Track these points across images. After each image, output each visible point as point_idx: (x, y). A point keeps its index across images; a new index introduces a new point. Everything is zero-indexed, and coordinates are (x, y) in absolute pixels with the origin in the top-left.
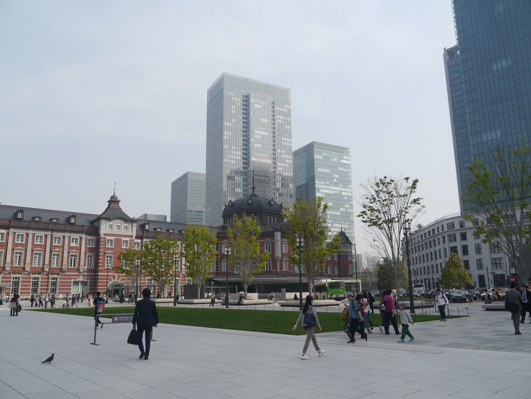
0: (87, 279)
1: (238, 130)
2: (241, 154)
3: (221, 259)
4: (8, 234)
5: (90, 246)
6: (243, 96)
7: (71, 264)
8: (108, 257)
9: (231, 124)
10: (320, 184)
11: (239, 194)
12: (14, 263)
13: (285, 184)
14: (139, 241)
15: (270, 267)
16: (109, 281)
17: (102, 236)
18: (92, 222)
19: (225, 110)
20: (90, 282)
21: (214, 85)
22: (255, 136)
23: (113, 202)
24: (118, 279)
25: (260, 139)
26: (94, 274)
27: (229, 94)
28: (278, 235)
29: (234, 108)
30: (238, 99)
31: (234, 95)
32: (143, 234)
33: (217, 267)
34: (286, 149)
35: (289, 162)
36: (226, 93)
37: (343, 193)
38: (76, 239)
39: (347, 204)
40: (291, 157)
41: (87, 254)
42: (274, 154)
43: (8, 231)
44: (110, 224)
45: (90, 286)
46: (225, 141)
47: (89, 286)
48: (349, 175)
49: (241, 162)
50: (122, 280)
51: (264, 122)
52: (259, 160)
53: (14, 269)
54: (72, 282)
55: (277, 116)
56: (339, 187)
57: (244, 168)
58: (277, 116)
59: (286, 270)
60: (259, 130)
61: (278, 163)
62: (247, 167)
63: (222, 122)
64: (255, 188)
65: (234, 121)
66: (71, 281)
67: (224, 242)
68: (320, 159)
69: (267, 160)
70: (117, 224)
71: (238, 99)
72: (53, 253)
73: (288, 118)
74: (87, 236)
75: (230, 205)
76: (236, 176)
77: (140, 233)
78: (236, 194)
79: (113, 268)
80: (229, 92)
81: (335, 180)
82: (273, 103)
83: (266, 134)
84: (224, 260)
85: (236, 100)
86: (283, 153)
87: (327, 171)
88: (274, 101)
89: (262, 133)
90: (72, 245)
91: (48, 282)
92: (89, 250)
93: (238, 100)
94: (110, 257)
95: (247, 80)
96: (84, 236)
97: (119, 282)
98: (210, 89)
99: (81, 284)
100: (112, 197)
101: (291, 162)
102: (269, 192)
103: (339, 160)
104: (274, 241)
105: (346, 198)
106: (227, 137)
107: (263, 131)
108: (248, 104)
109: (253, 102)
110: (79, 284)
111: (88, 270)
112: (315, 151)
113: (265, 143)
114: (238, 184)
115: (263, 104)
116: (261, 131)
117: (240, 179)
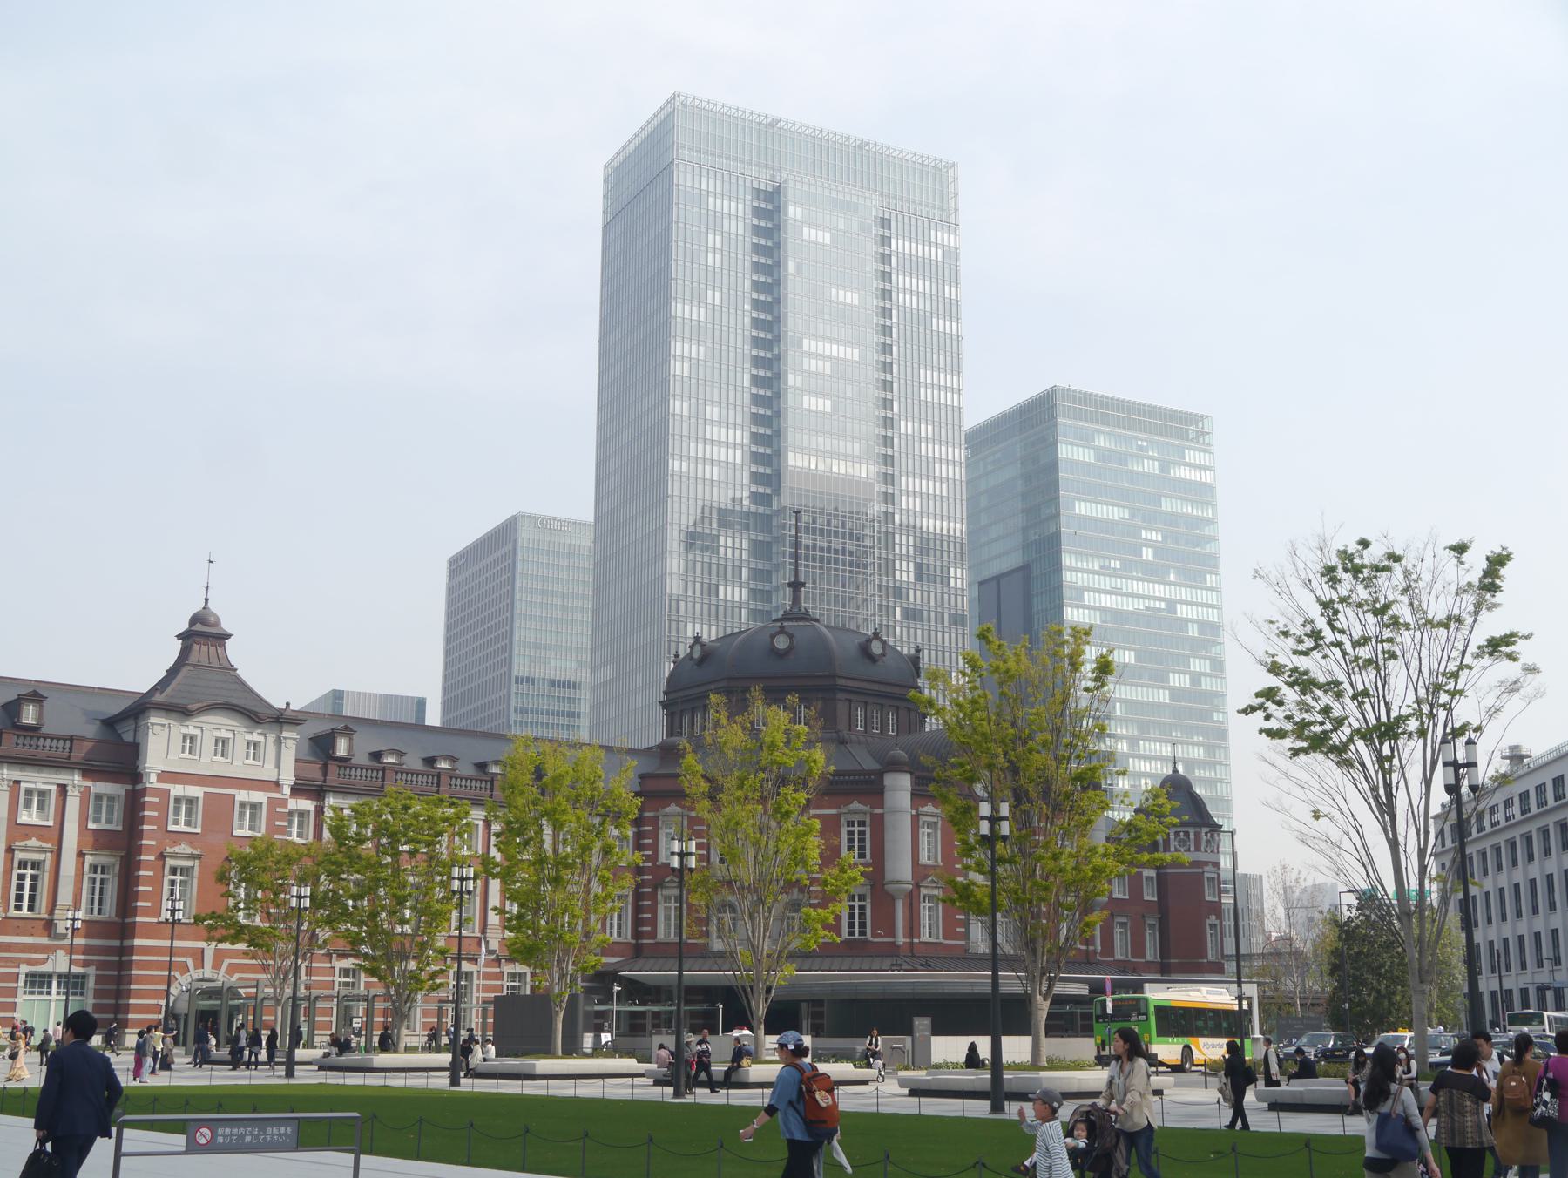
0: (86, 964)
1: (732, 336)
2: (747, 441)
3: (655, 889)
5: (103, 826)
6: (757, 193)
7: (19, 898)
8: (174, 871)
9: (702, 311)
10: (1083, 571)
11: (737, 610)
13: (932, 568)
14: (308, 805)
15: (863, 925)
16: (177, 974)
17: (152, 781)
18: (110, 723)
19: (678, 252)
20: (99, 979)
21: (632, 146)
22: (806, 361)
23: (197, 639)
24: (217, 965)
25: (824, 375)
26: (116, 943)
27: (696, 186)
28: (900, 787)
29: (718, 246)
30: (733, 204)
31: (718, 190)
32: (325, 774)
33: (637, 922)
34: (936, 419)
35: (951, 476)
36: (681, 182)
37: (1182, 611)
38: (43, 794)
39: (1200, 657)
40: (959, 454)
41: (89, 859)
42: (887, 441)
44: (185, 730)
45: (98, 994)
46: (678, 384)
47: (90, 994)
48: (1208, 531)
49: (746, 475)
50: (233, 969)
51: (845, 304)
52: (821, 467)
54: (22, 978)
55: (901, 278)
56: (1164, 583)
57: (755, 498)
58: (900, 280)
59: (931, 940)
60: (824, 339)
61: (903, 479)
62: (769, 497)
63: (666, 304)
64: (803, 584)
65: (714, 297)
67: (666, 815)
68: (1084, 463)
69: (857, 465)
70: (217, 734)
71: (733, 204)
73: (947, 288)
74: (89, 783)
75: (697, 654)
76: (722, 533)
77: (314, 772)
78: (721, 609)
79: (198, 920)
80: (697, 178)
81: (1148, 554)
82: (885, 223)
83: (854, 354)
84: (667, 892)
85: (726, 211)
86: (923, 434)
87: (1113, 513)
88: (887, 216)
89: (834, 350)
90: (24, 818)
92: (96, 840)
93: (733, 212)
94: (186, 871)
95: (771, 125)
96: (75, 780)
97: (221, 978)
98: (615, 164)
99: (59, 986)
100: (194, 620)
101: (959, 473)
102: (861, 602)
103: (1165, 467)
104: (882, 815)
105: (1193, 631)
106: (686, 365)
107: (838, 342)
108: (778, 227)
109: (799, 217)
110: (50, 986)
111: (92, 928)
112: (1060, 429)
113: (849, 394)
114: (729, 569)
115: (841, 227)
116: (831, 340)
117: (737, 545)
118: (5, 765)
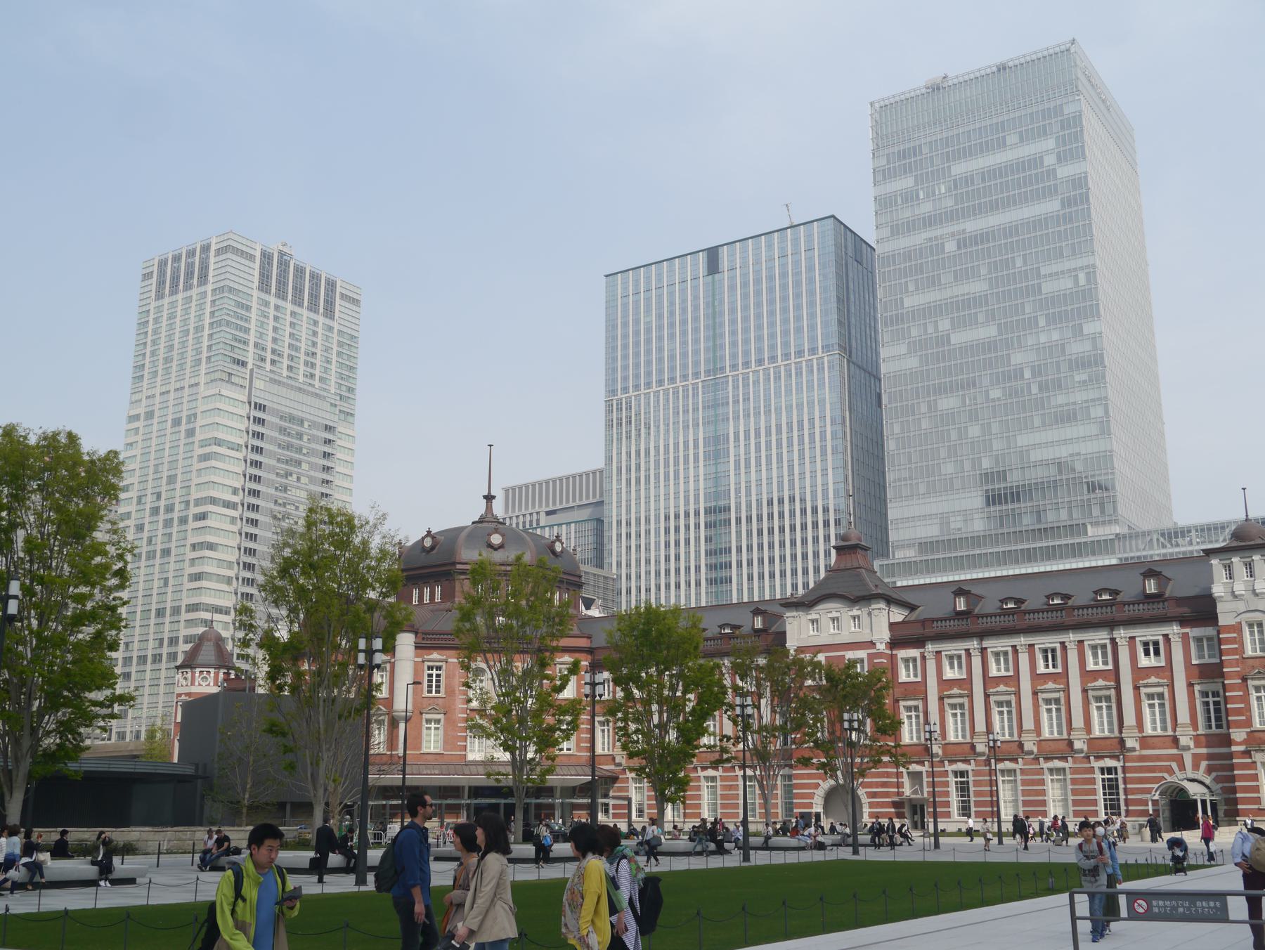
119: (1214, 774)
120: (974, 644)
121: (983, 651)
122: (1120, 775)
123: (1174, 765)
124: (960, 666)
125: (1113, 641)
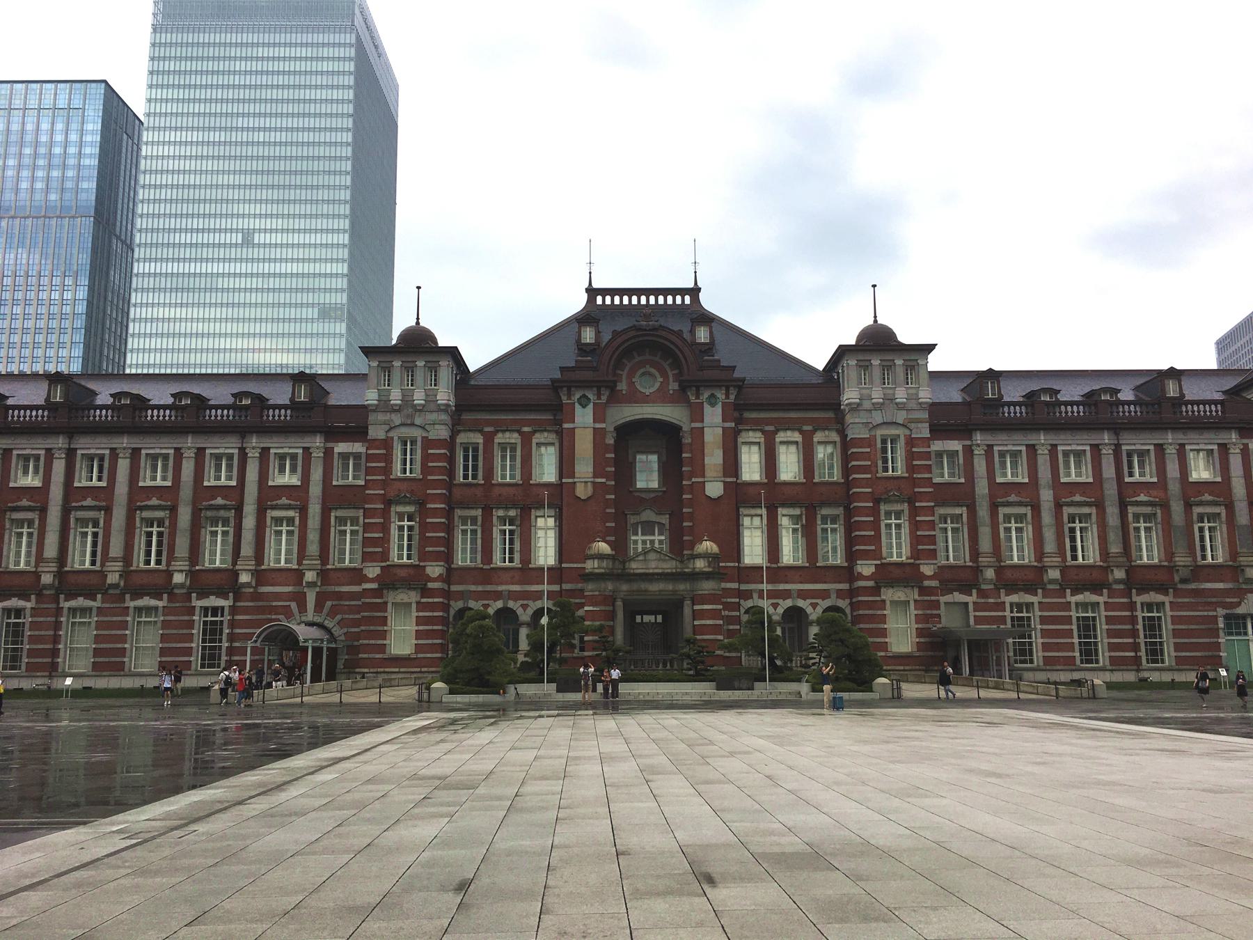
4: (969, 451)
12: (1005, 553)
43: (968, 443)
53: (1008, 574)
66: (1215, 613)
72: (1131, 510)
91: (1133, 620)
110: (1245, 627)
118: (1169, 431)
119: (339, 617)
120: (60, 442)
121: (71, 454)
122: (227, 617)
123: (293, 605)
124: (36, 471)
125: (242, 451)
